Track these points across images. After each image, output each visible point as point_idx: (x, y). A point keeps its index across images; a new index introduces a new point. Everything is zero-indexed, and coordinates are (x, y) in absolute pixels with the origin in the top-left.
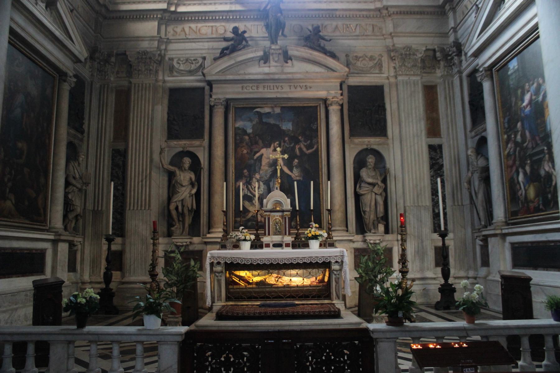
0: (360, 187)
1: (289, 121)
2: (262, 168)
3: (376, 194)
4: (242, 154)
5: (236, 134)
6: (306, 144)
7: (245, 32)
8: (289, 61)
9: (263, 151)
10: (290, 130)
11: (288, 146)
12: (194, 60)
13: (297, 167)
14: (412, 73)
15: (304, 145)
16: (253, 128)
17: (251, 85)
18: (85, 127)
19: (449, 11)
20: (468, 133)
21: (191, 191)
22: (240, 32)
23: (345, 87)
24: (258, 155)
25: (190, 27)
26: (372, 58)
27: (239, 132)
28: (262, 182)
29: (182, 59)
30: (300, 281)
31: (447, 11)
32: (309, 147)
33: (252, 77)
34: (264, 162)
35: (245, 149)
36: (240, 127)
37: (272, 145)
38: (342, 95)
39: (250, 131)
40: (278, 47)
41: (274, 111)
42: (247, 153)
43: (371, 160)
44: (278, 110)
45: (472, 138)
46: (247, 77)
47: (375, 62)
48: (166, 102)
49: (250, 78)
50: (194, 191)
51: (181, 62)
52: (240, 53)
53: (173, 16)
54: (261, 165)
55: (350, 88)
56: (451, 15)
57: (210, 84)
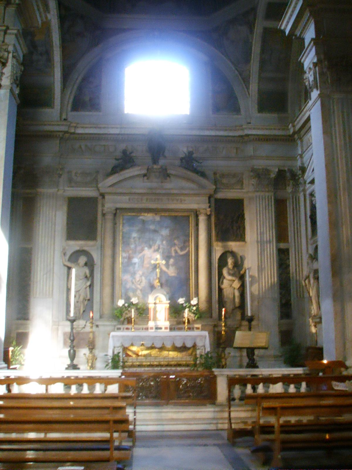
0: (222, 282)
3: (234, 288)
7: (131, 153)
8: (168, 178)
13: (172, 265)
14: (267, 190)
15: (178, 247)
19: (297, 139)
20: (309, 240)
22: (128, 153)
23: (212, 200)
25: (86, 146)
26: (234, 176)
30: (175, 354)
31: (296, 139)
37: (153, 247)
38: (210, 207)
40: (159, 167)
43: (230, 261)
45: (312, 244)
50: (89, 283)
52: (127, 171)
53: (72, 136)
55: (217, 200)
56: (299, 142)
57: (103, 195)
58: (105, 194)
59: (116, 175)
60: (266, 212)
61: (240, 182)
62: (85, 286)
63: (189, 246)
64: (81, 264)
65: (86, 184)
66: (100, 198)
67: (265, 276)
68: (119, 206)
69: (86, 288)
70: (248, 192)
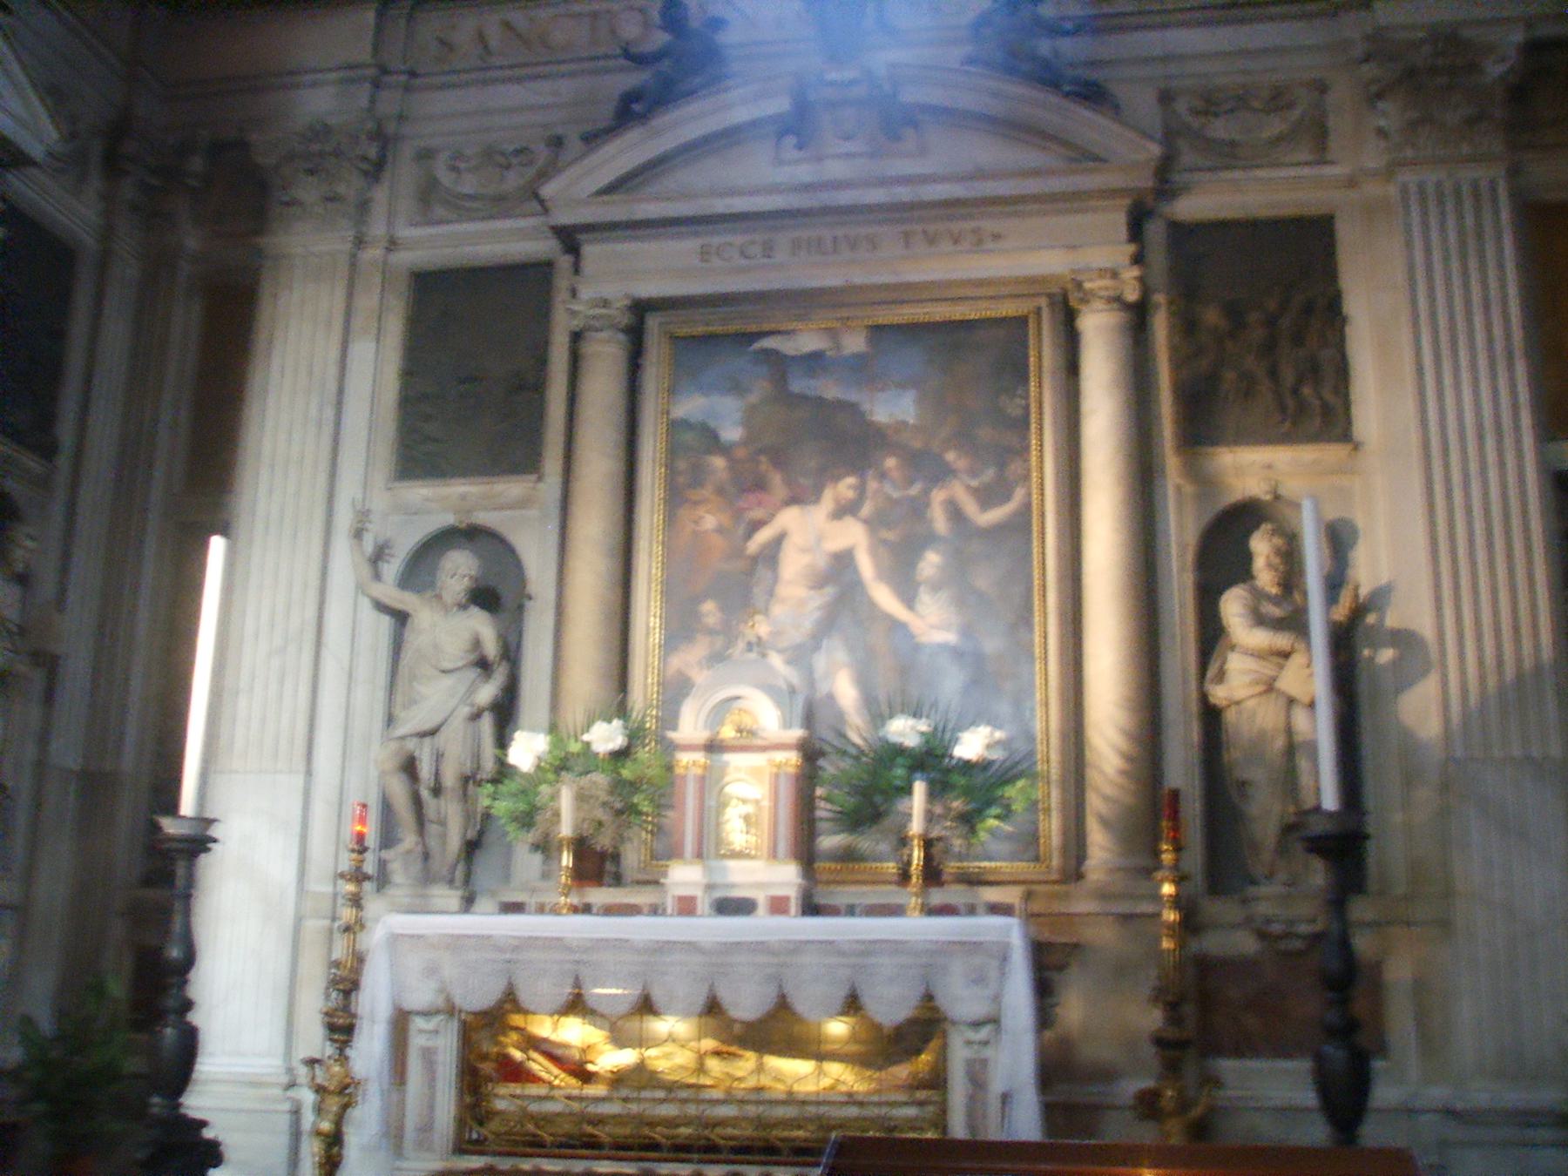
1: (902, 386)
2: (783, 590)
3: (1291, 701)
4: (695, 533)
5: (673, 451)
6: (974, 483)
9: (787, 517)
10: (904, 423)
11: (896, 495)
12: (518, 152)
13: (936, 587)
15: (968, 487)
16: (747, 421)
17: (738, 239)
18: (66, 433)
21: (472, 690)
24: (763, 536)
25: (508, 25)
26: (1278, 100)
27: (688, 437)
28: (780, 651)
29: (468, 152)
32: (987, 497)
33: (740, 204)
34: (793, 564)
35: (708, 512)
36: (692, 420)
38: (1138, 259)
39: (732, 433)
41: (838, 347)
42: (720, 530)
44: (855, 343)
46: (721, 206)
47: (1296, 114)
48: (395, 327)
49: (734, 210)
50: (487, 692)
51: (463, 166)
54: (776, 579)
55: (1181, 232)
57: (570, 239)
58: (582, 237)
59: (633, 135)
60: (1465, 274)
61: (1316, 134)
62: (465, 711)
63: (1026, 477)
64: (449, 598)
65: (500, 205)
66: (565, 261)
67: (1479, 638)
68: (649, 289)
69: (476, 716)
70: (1351, 183)
